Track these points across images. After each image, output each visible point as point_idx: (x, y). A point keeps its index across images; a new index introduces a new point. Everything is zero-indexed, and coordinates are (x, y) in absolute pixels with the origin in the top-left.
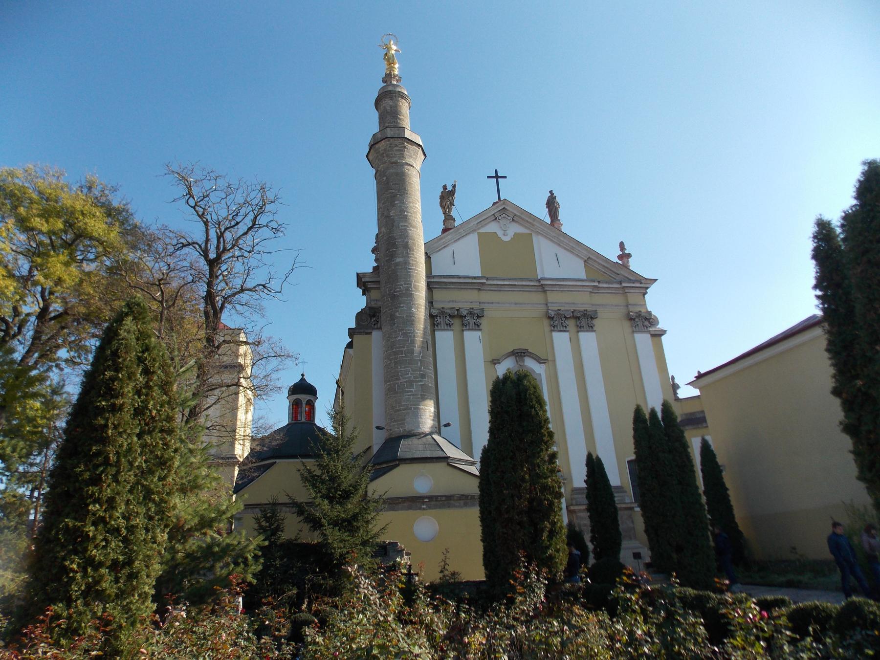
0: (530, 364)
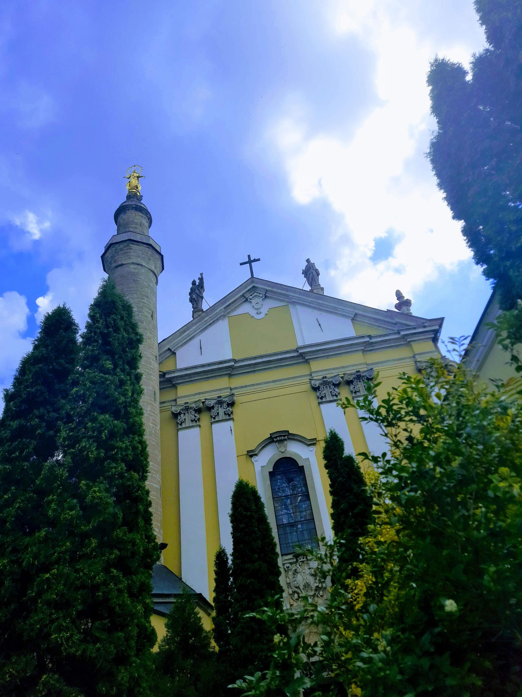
0: (294, 449)
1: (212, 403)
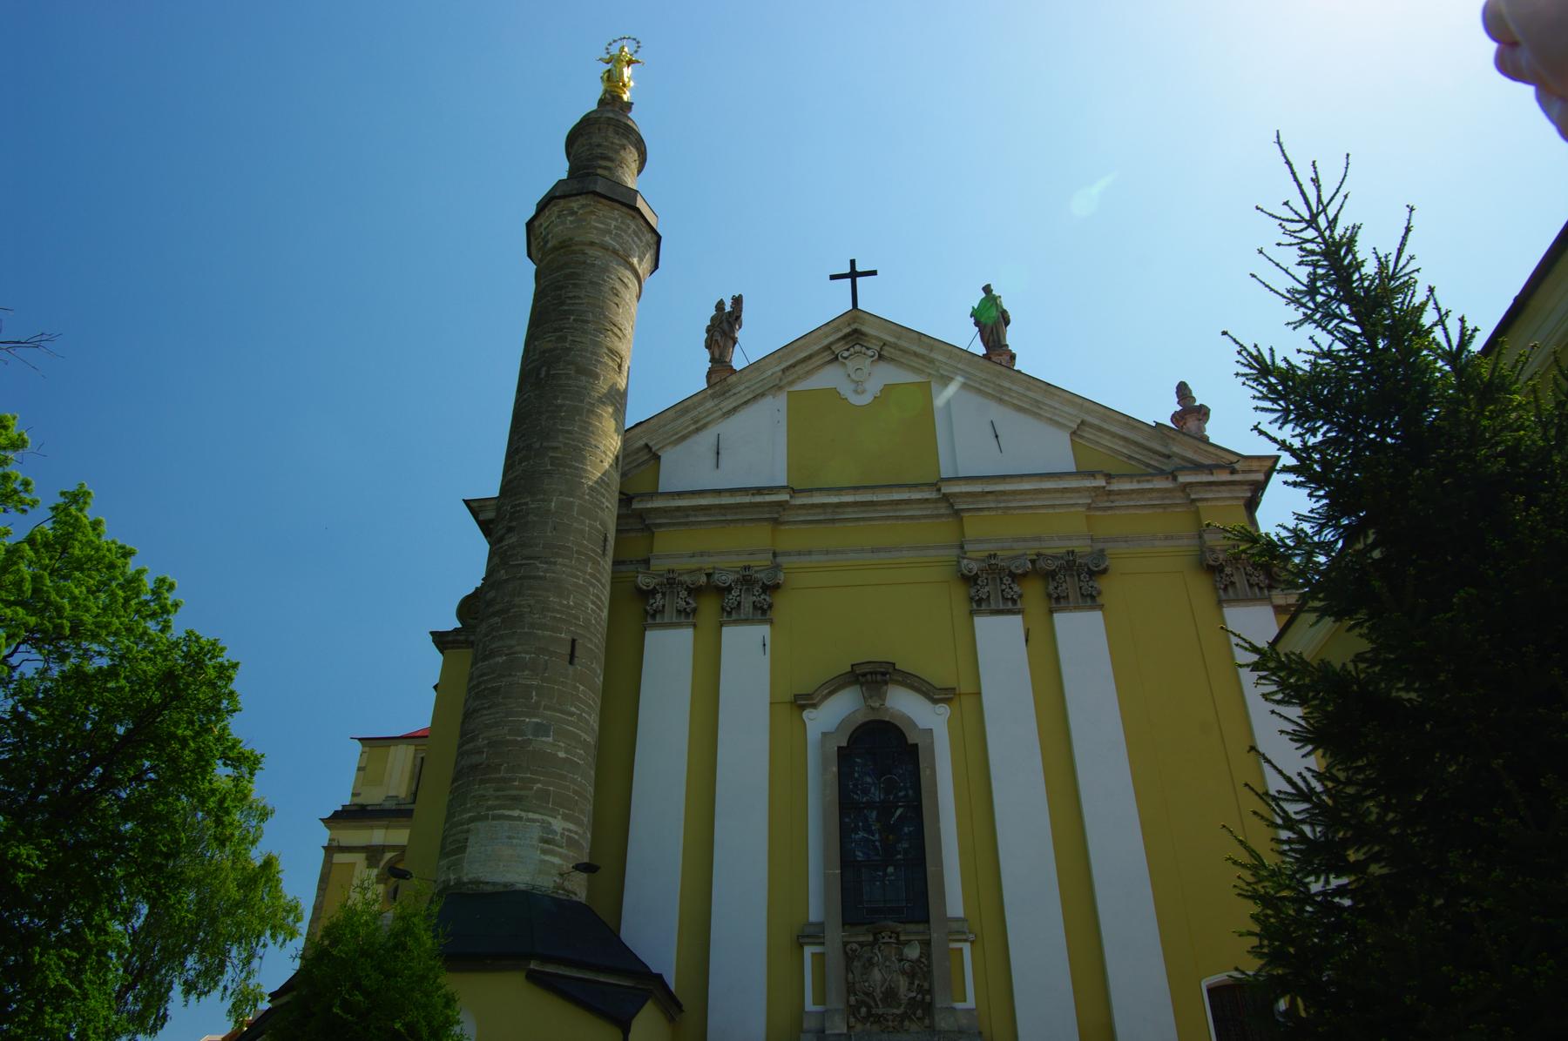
0: (904, 704)
1: (729, 578)
